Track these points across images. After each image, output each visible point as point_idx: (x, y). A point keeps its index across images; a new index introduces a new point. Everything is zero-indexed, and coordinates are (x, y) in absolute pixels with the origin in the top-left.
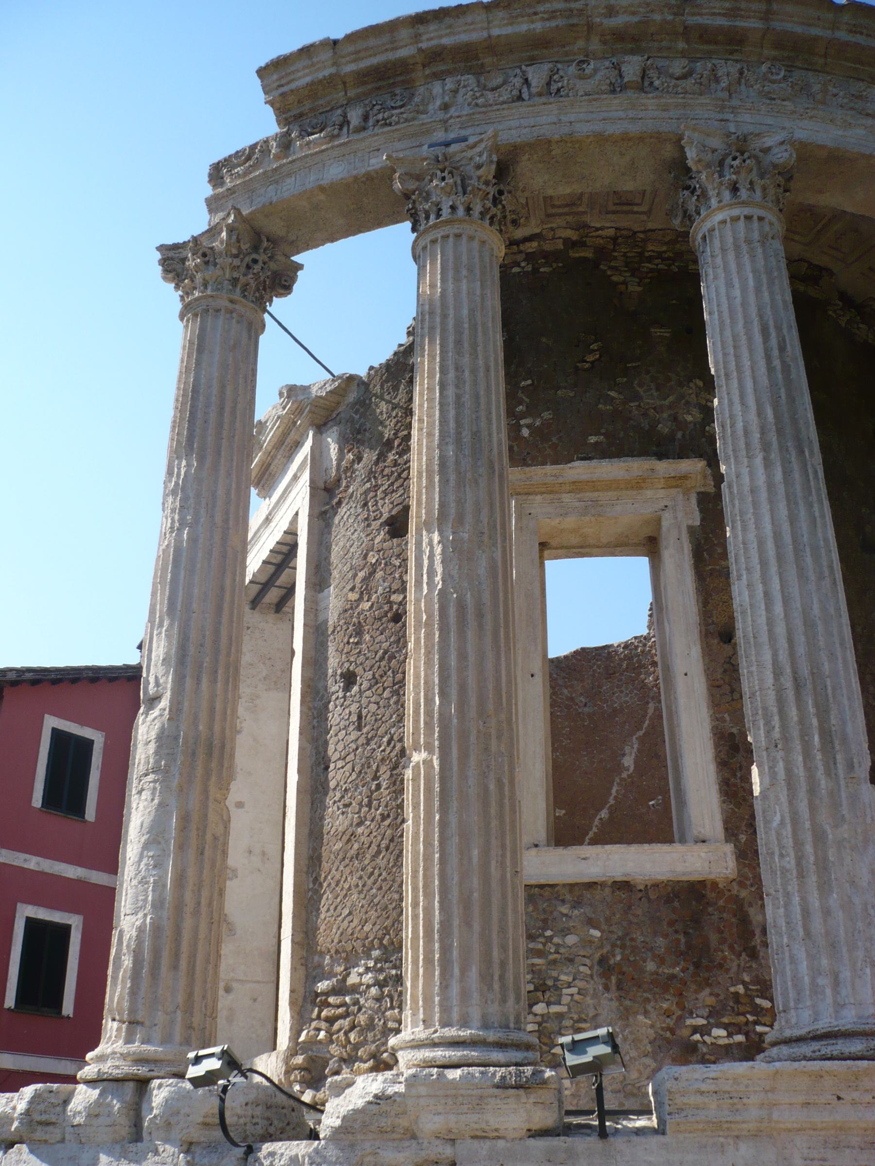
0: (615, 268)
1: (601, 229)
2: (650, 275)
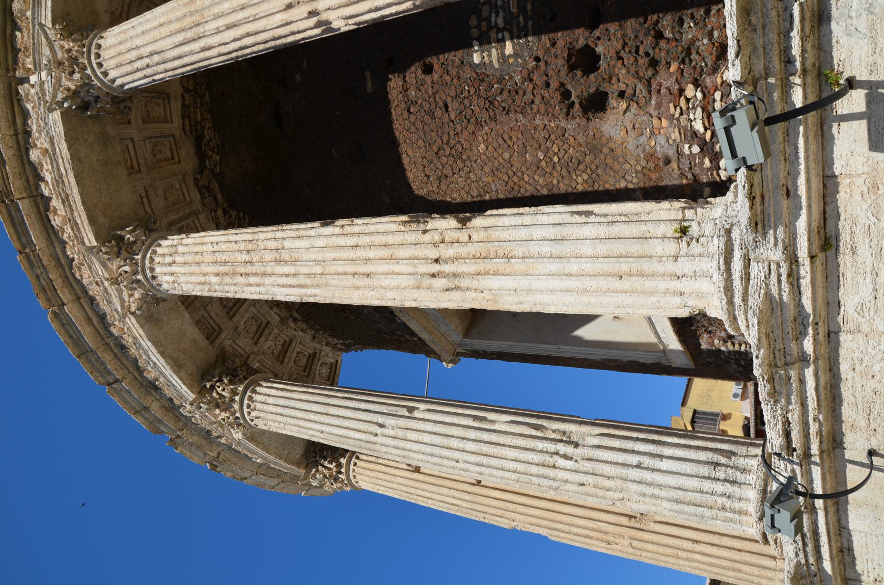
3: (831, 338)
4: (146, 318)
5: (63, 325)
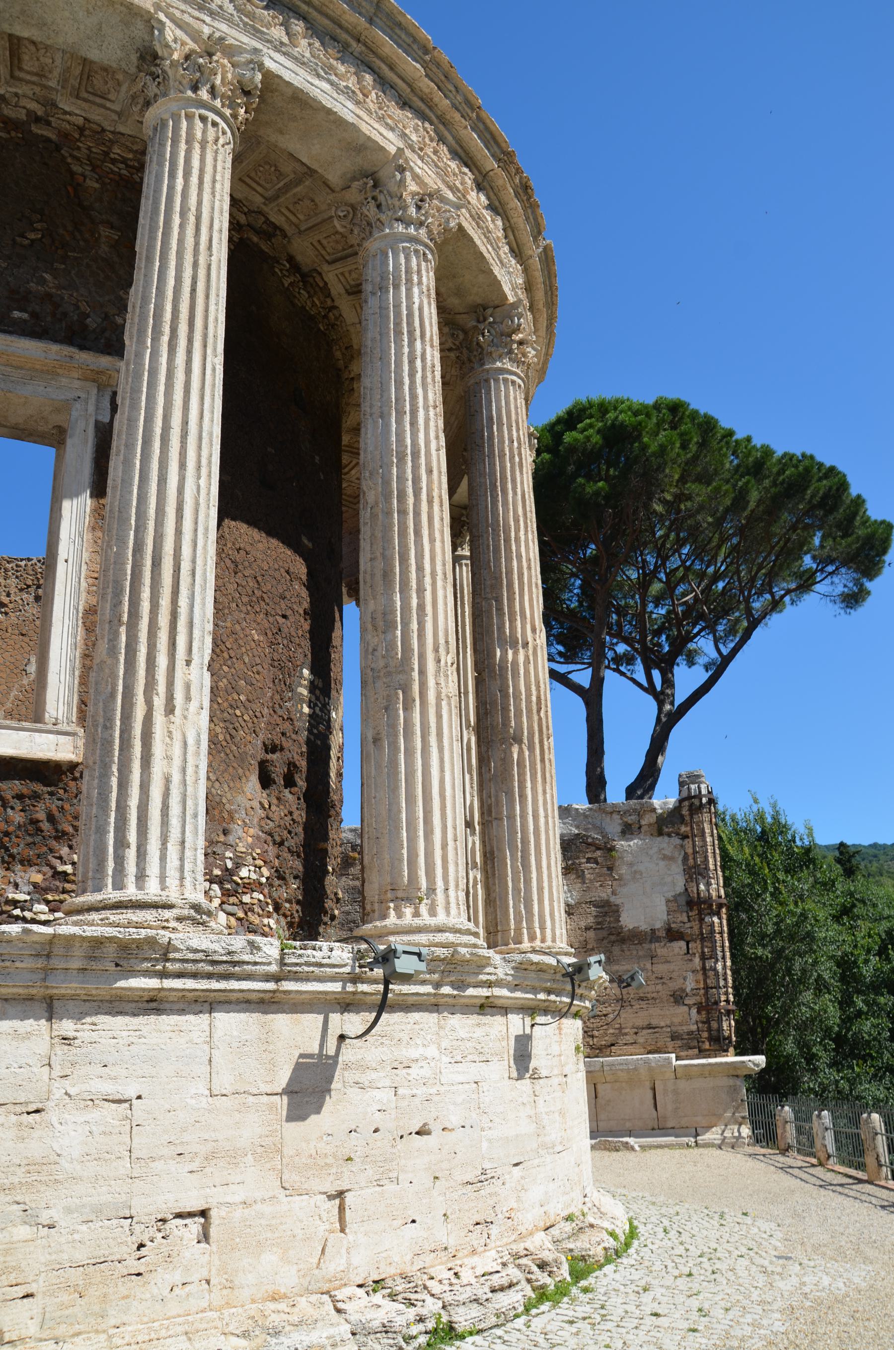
0: (78, 159)
2: (111, 176)
3: (434, 1006)
4: (366, 148)
5: (415, 40)
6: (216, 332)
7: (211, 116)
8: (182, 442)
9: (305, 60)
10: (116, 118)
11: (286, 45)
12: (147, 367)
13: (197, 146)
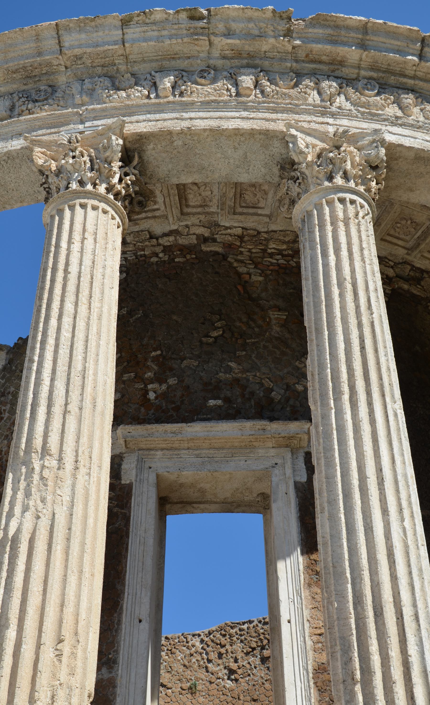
0: (242, 262)
1: (230, 228)
6: (390, 380)
7: (349, 196)
8: (379, 489)
9: (421, 124)
10: (267, 220)
11: (400, 118)
12: (334, 426)
13: (341, 225)
